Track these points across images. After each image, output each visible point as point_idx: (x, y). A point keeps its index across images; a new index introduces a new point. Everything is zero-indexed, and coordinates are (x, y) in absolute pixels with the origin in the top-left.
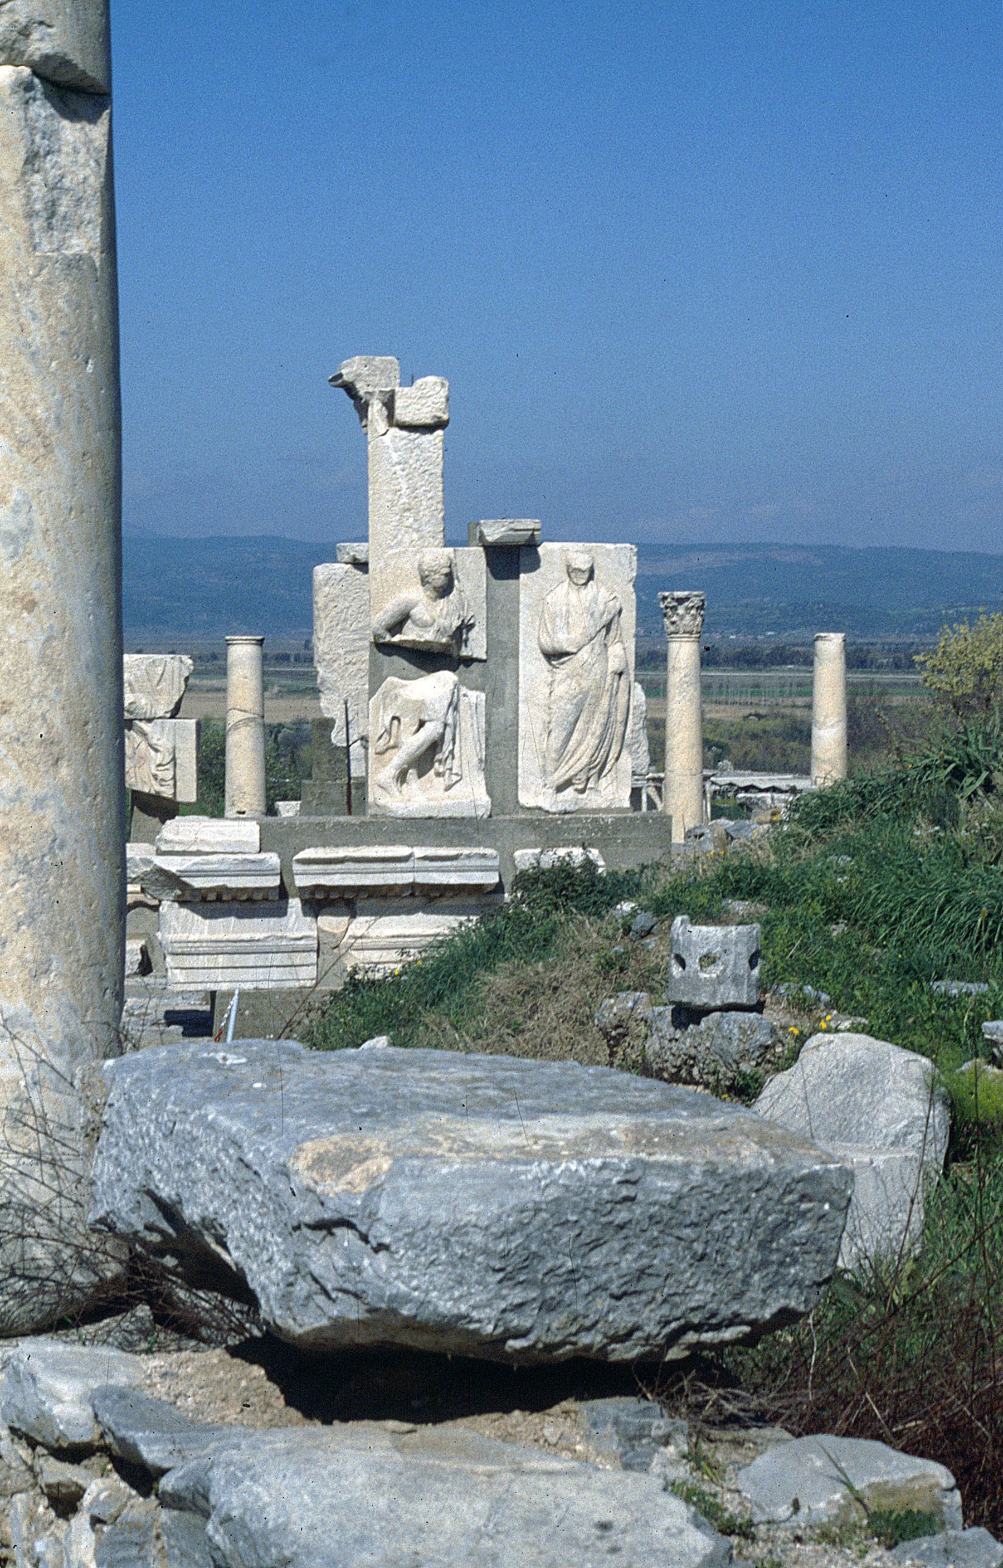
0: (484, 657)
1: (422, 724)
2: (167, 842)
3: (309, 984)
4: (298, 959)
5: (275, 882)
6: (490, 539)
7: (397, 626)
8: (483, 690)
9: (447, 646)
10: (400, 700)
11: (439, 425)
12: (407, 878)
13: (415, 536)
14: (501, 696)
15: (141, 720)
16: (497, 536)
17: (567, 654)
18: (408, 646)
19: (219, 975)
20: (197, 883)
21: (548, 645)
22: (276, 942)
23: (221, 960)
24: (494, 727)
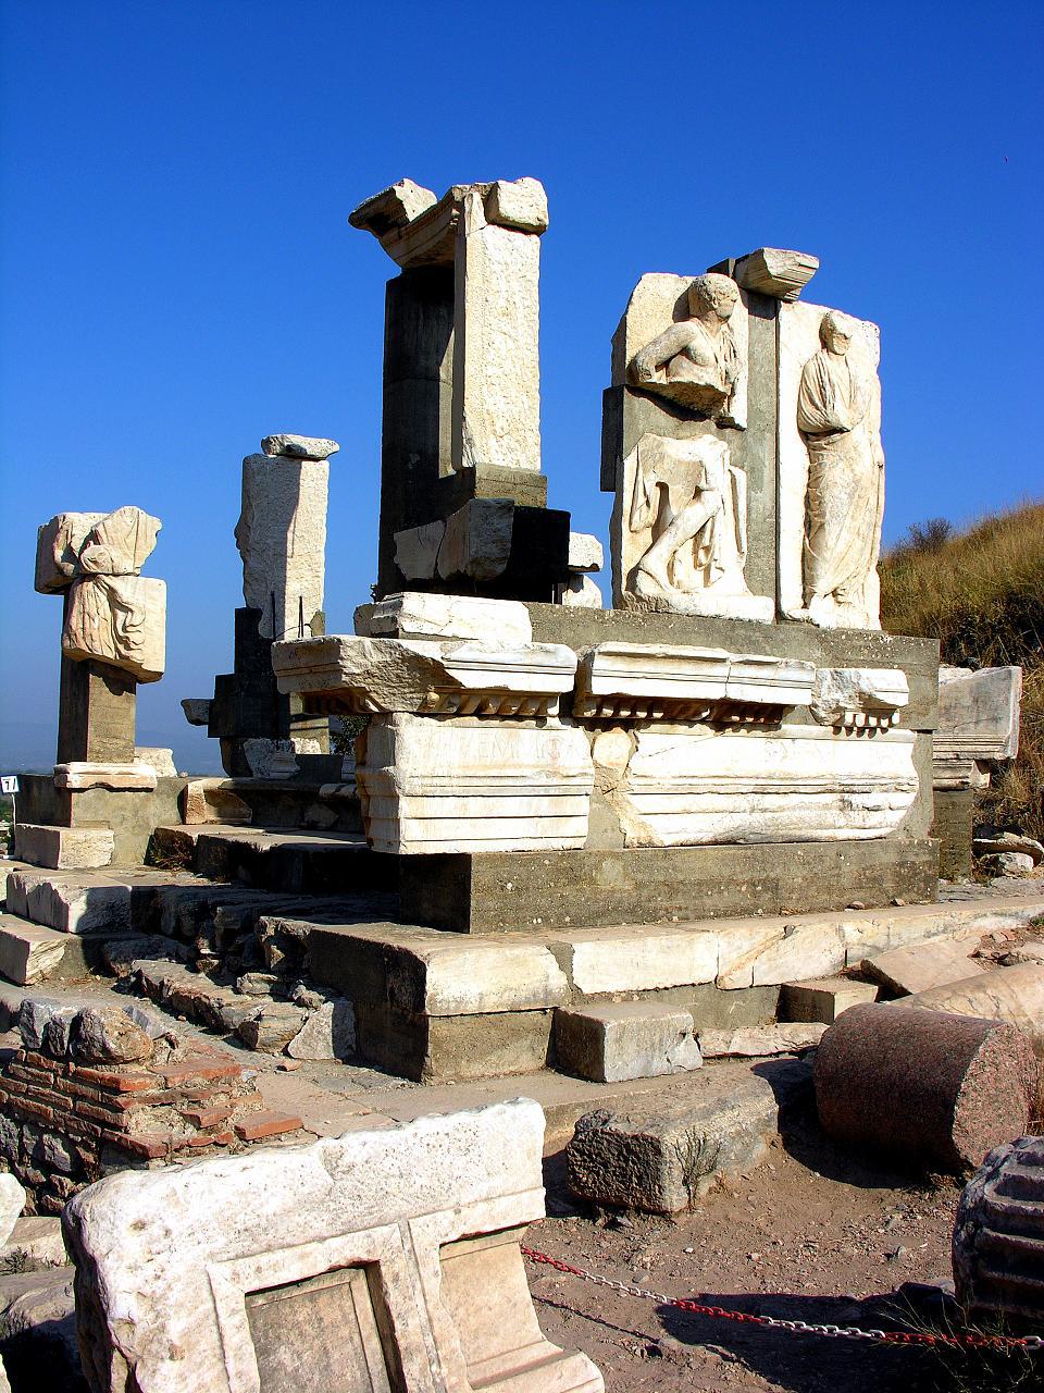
0: (745, 426)
1: (698, 492)
2: (412, 617)
3: (579, 843)
4: (568, 805)
5: (566, 684)
6: (773, 272)
7: (664, 365)
8: (742, 468)
9: (723, 395)
10: (666, 460)
11: (537, 230)
12: (715, 692)
13: (511, 345)
14: (763, 474)
15: (107, 575)
16: (780, 271)
17: (841, 431)
18: (670, 394)
19: (465, 830)
20: (470, 680)
21: (815, 417)
22: (544, 781)
23: (476, 806)
24: (754, 516)
